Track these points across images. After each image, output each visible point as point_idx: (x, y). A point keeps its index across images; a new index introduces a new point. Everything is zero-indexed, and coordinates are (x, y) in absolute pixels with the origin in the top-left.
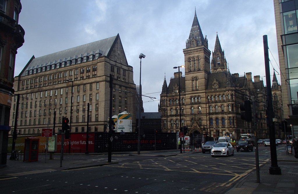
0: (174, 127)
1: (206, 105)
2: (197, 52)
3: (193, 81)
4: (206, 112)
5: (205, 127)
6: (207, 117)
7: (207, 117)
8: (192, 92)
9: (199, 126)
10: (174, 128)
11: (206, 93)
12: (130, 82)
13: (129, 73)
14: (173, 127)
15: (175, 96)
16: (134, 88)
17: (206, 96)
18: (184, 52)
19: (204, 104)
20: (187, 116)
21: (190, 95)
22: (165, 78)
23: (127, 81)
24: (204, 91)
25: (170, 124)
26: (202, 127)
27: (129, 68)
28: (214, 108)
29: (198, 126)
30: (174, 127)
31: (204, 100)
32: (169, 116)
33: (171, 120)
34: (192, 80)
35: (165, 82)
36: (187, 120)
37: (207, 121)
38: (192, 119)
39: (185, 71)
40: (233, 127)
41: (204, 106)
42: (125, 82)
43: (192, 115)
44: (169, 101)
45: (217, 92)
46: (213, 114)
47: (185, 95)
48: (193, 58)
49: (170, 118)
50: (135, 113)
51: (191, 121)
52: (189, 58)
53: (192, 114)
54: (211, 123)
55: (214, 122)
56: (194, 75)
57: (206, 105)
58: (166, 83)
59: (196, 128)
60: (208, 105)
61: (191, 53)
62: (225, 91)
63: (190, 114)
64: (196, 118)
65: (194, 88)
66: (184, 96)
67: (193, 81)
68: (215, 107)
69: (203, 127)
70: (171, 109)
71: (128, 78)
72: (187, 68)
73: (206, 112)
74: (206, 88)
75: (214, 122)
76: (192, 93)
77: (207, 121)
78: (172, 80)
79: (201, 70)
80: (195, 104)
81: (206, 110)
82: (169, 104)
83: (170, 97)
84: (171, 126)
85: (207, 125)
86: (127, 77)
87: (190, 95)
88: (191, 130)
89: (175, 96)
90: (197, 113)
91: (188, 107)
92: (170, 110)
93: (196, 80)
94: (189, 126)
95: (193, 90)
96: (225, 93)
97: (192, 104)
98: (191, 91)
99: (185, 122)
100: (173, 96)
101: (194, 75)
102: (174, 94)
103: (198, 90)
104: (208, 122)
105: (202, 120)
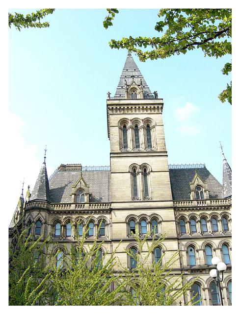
2: (145, 112)
11: (175, 208)
17: (176, 218)
18: (111, 107)
24: (171, 204)
31: (168, 228)
35: (45, 171)
41: (174, 245)
47: (111, 210)
48: (136, 121)
52: (123, 122)
61: (130, 112)
65: (140, 195)
66: (108, 216)
68: (204, 251)
76: (133, 207)
81: (180, 258)
98: (131, 200)
101: (140, 161)
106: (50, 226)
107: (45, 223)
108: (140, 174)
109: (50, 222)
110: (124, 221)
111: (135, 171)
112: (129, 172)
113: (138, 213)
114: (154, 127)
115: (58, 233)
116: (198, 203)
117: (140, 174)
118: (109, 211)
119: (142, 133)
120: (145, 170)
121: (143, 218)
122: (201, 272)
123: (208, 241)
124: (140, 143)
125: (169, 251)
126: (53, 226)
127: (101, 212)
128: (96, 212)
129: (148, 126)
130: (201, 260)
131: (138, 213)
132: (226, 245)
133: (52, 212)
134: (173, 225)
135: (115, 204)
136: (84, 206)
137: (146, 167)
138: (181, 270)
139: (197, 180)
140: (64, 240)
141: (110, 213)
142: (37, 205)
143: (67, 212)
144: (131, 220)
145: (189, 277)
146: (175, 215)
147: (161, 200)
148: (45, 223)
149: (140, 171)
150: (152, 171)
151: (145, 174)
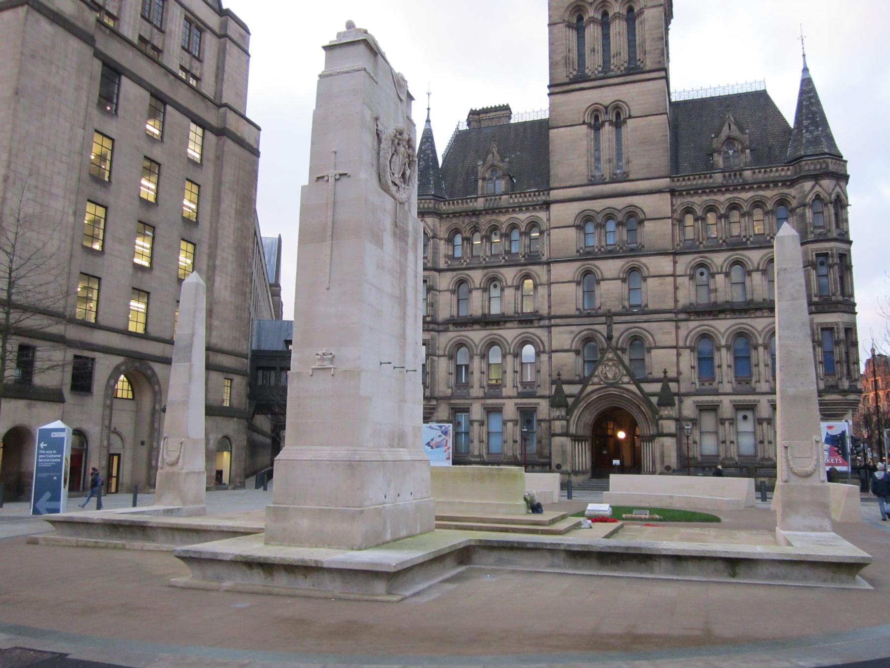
0: (476, 385)
1: (675, 263)
3: (596, 127)
4: (676, 301)
5: (673, 386)
6: (677, 328)
7: (677, 328)
8: (590, 188)
9: (637, 382)
10: (476, 391)
11: (673, 192)
12: (224, 101)
13: (222, 54)
14: (468, 385)
15: (487, 211)
16: (252, 142)
17: (673, 211)
19: (665, 253)
20: (558, 321)
21: (575, 208)
22: (428, 121)
23: (208, 88)
24: (664, 182)
25: (452, 369)
26: (656, 387)
27: (224, 26)
28: (720, 278)
29: (626, 379)
30: (476, 385)
32: (447, 322)
33: (460, 345)
34: (590, 126)
36: (555, 345)
37: (678, 355)
38: (587, 340)
39: (551, 74)
40: (846, 384)
41: (664, 264)
42: (196, 91)
43: (589, 316)
44: (450, 241)
45: (745, 186)
46: (715, 311)
47: (546, 205)
49: (450, 335)
50: (244, 294)
51: (577, 352)
53: (584, 315)
54: (705, 363)
55: (724, 358)
56: (606, 96)
57: (675, 263)
58: (433, 145)
59: (613, 391)
60: (685, 262)
62: (791, 182)
63: (573, 312)
64: (615, 334)
66: (542, 215)
67: (596, 127)
68: (727, 275)
69: (656, 387)
70: (461, 282)
71: (217, 76)
72: (559, 58)
73: (676, 301)
74: (675, 168)
75: (724, 358)
76: (589, 195)
77: (678, 355)
78: (460, 139)
79: (648, 68)
80: (611, 254)
81: (676, 288)
82: (447, 256)
83: (455, 220)
84: (453, 379)
85: (679, 373)
86: (208, 70)
87: (575, 208)
88: (582, 405)
89: (487, 211)
90: (619, 309)
91: (566, 271)
92: (453, 292)
93: (611, 123)
94: (571, 382)
95: (591, 183)
96: (793, 192)
97: (587, 255)
98: (585, 182)
99: (544, 357)
100: (475, 213)
101: (606, 96)
102: (480, 204)
103: (625, 179)
104: (688, 360)
105: (649, 350)
106: (442, 242)
107: (433, 238)
108: (607, 124)
109: (442, 233)
110: (572, 224)
111: (596, 118)
112: (584, 123)
113: (598, 205)
114: (641, 12)
115: (458, 253)
116: (724, 176)
117: (607, 124)
118: (545, 207)
119: (618, 28)
120: (618, 115)
121: (609, 217)
122: (714, 315)
123: (463, 274)
124: (612, 54)
125: (654, 276)
126: (450, 241)
127: (531, 208)
128: (520, 208)
129: (630, 10)
130: (718, 294)
131: (598, 205)
132: (634, 270)
133: (445, 216)
134: (666, 226)
135: (555, 191)
136: (500, 199)
137: (620, 108)
138: (677, 313)
139: (726, 127)
140: (467, 264)
141: (548, 209)
142: (426, 206)
143: (470, 213)
144: (584, 221)
145: (692, 324)
146: (672, 205)
147: (645, 176)
148: (433, 238)
149: (607, 118)
150: (630, 117)
151: (618, 124)
